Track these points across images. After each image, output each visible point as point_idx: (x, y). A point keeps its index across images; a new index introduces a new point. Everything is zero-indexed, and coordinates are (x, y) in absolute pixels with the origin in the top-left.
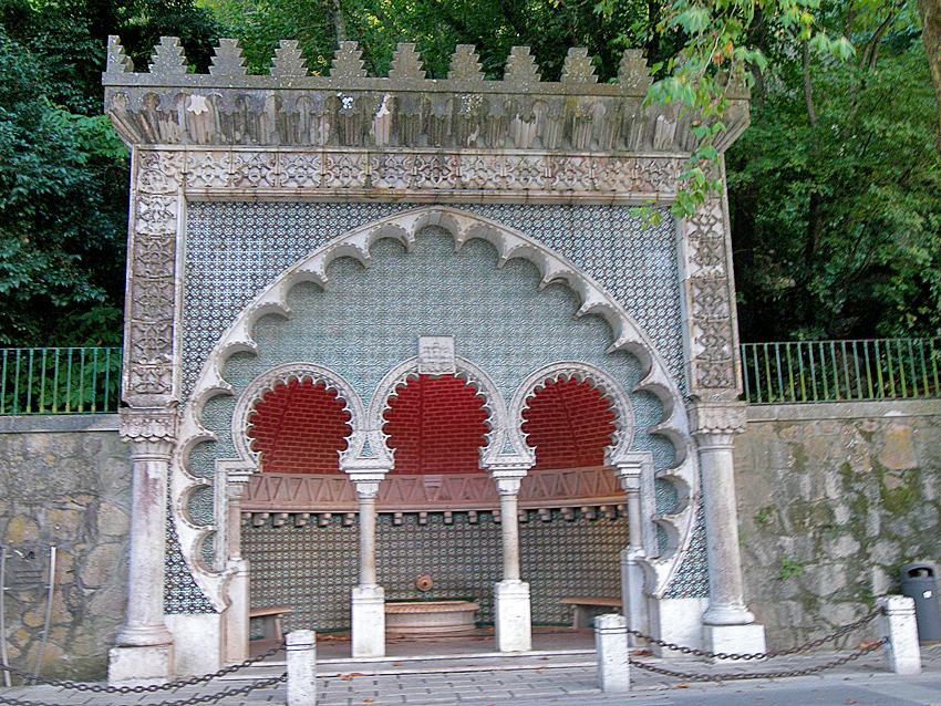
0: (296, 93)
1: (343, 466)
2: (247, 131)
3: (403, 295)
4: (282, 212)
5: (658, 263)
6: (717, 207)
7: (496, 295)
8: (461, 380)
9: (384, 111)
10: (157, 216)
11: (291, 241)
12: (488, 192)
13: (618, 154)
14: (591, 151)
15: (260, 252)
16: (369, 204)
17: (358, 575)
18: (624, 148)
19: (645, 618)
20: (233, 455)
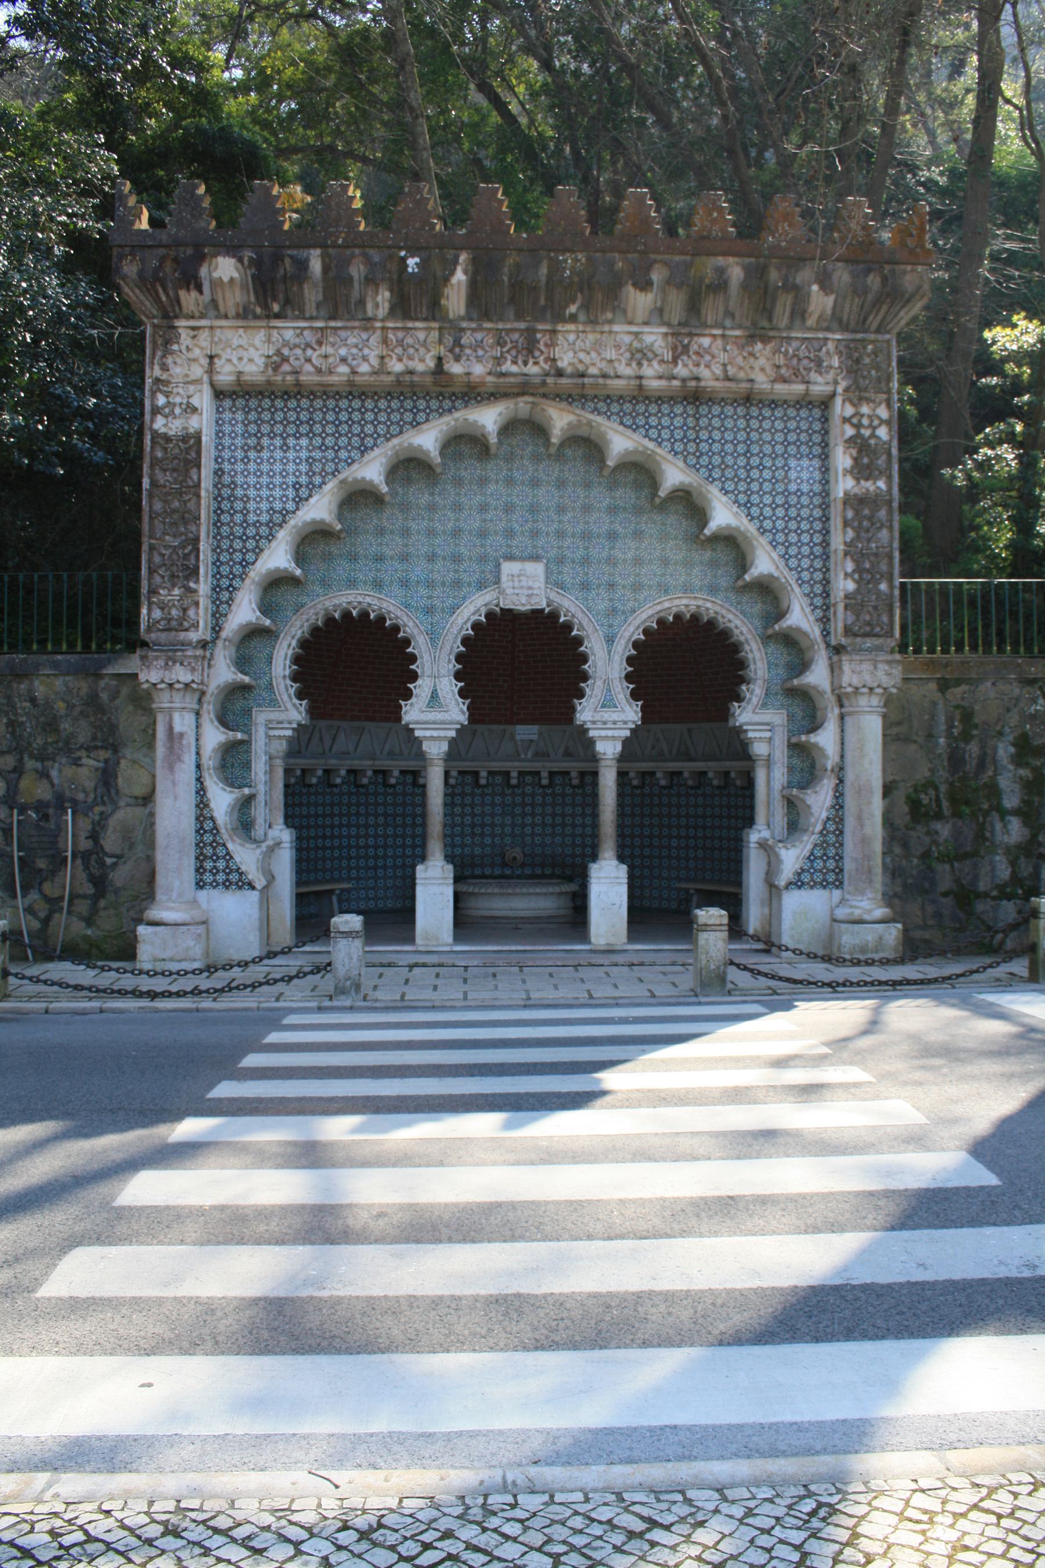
0: (348, 252)
2: (287, 302)
3: (483, 508)
4: (331, 403)
6: (883, 406)
7: (599, 510)
8: (554, 615)
9: (460, 276)
10: (177, 411)
11: (343, 441)
12: (591, 380)
13: (758, 332)
14: (724, 328)
15: (304, 454)
16: (441, 394)
17: (424, 845)
18: (765, 323)
19: (766, 911)
20: (274, 703)
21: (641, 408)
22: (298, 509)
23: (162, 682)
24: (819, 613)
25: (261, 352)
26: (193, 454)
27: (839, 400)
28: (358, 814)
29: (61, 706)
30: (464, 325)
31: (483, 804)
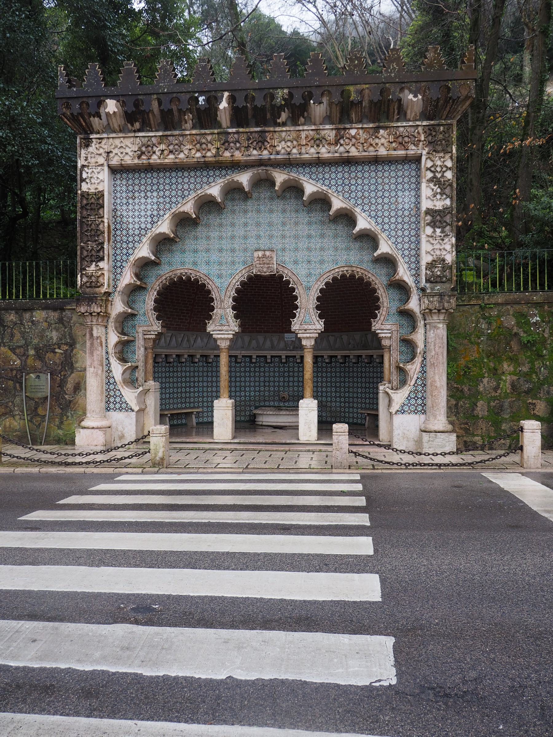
0: (171, 96)
1: (208, 329)
3: (246, 225)
5: (407, 200)
7: (303, 224)
9: (224, 105)
12: (294, 156)
15: (155, 200)
17: (218, 392)
21: (320, 169)
22: (152, 227)
23: (87, 312)
24: (413, 272)
25: (131, 149)
26: (101, 201)
27: (424, 158)
28: (207, 376)
29: (45, 324)
30: (230, 130)
31: (269, 372)
